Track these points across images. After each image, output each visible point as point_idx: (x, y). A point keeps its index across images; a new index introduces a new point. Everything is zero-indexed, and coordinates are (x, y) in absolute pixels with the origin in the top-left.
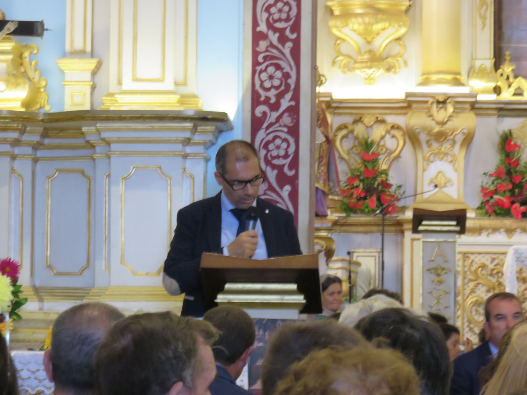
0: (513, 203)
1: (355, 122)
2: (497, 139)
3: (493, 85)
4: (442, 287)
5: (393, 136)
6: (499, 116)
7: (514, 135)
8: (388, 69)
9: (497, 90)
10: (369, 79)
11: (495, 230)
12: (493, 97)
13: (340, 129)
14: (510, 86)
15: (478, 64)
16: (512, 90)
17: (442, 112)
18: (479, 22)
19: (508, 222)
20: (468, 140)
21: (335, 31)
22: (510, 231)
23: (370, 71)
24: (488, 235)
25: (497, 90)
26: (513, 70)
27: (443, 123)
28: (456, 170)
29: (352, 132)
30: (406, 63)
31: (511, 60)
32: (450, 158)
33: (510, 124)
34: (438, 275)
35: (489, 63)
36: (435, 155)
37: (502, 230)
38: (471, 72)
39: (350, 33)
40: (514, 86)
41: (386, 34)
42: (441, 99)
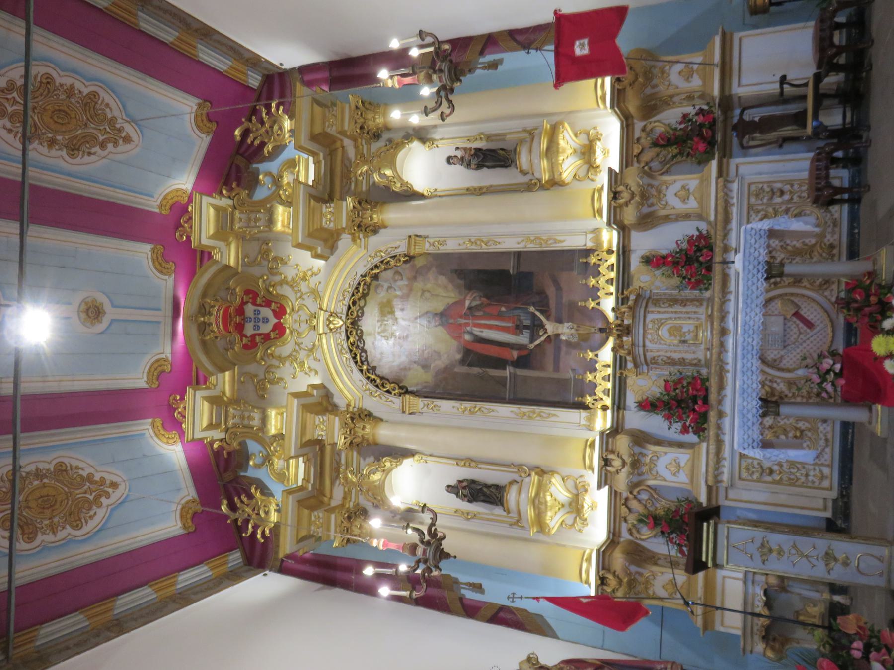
0: (694, 410)
1: (626, 520)
2: (643, 413)
3: (600, 413)
4: (786, 548)
5: (639, 493)
6: (624, 409)
7: (640, 399)
8: (586, 491)
9: (605, 408)
10: (593, 507)
11: (719, 427)
12: (609, 412)
13: (631, 534)
14: (602, 399)
15: (583, 422)
16: (605, 397)
17: (614, 463)
18: (553, 419)
19: (712, 415)
20: (640, 439)
21: (553, 531)
22: (721, 415)
23: (586, 506)
24: (724, 434)
25: (605, 408)
26: (590, 396)
27: (624, 463)
28: (665, 453)
29: (634, 525)
30: (581, 476)
31: (583, 396)
32: (655, 458)
33: (631, 399)
34: (771, 551)
35: (584, 414)
36: (651, 470)
37: (719, 422)
38: (590, 428)
39: (554, 519)
40: (601, 395)
41: (558, 491)
42: (603, 463)
